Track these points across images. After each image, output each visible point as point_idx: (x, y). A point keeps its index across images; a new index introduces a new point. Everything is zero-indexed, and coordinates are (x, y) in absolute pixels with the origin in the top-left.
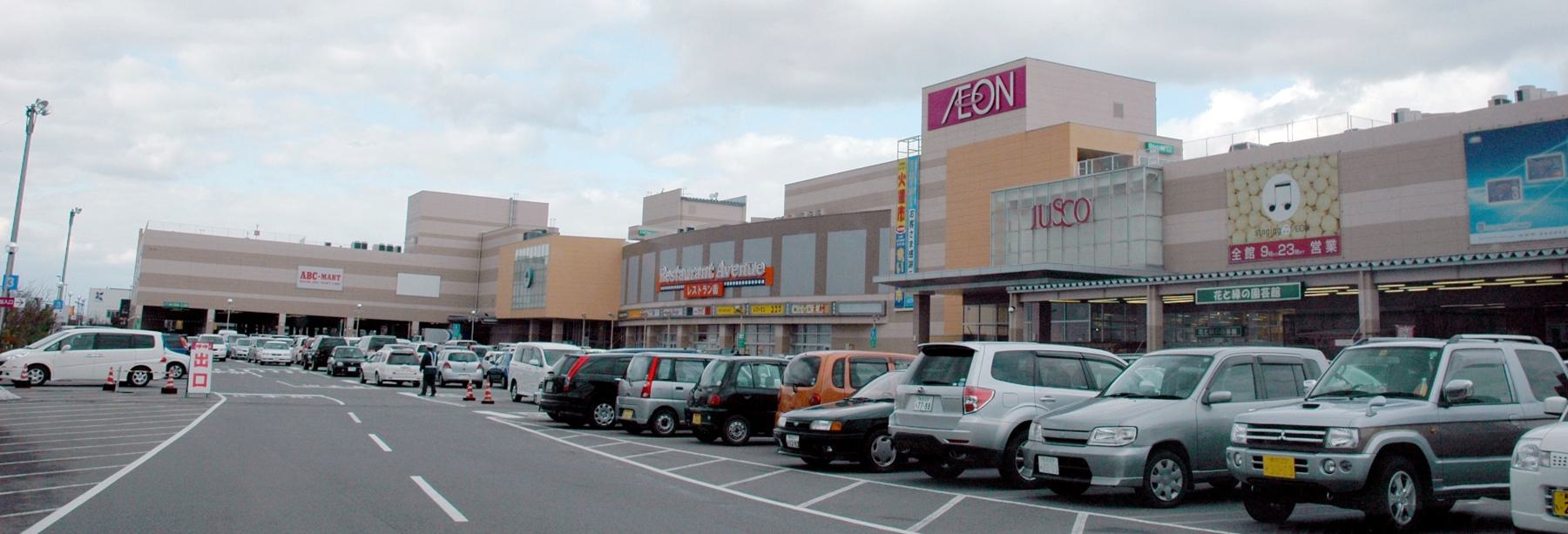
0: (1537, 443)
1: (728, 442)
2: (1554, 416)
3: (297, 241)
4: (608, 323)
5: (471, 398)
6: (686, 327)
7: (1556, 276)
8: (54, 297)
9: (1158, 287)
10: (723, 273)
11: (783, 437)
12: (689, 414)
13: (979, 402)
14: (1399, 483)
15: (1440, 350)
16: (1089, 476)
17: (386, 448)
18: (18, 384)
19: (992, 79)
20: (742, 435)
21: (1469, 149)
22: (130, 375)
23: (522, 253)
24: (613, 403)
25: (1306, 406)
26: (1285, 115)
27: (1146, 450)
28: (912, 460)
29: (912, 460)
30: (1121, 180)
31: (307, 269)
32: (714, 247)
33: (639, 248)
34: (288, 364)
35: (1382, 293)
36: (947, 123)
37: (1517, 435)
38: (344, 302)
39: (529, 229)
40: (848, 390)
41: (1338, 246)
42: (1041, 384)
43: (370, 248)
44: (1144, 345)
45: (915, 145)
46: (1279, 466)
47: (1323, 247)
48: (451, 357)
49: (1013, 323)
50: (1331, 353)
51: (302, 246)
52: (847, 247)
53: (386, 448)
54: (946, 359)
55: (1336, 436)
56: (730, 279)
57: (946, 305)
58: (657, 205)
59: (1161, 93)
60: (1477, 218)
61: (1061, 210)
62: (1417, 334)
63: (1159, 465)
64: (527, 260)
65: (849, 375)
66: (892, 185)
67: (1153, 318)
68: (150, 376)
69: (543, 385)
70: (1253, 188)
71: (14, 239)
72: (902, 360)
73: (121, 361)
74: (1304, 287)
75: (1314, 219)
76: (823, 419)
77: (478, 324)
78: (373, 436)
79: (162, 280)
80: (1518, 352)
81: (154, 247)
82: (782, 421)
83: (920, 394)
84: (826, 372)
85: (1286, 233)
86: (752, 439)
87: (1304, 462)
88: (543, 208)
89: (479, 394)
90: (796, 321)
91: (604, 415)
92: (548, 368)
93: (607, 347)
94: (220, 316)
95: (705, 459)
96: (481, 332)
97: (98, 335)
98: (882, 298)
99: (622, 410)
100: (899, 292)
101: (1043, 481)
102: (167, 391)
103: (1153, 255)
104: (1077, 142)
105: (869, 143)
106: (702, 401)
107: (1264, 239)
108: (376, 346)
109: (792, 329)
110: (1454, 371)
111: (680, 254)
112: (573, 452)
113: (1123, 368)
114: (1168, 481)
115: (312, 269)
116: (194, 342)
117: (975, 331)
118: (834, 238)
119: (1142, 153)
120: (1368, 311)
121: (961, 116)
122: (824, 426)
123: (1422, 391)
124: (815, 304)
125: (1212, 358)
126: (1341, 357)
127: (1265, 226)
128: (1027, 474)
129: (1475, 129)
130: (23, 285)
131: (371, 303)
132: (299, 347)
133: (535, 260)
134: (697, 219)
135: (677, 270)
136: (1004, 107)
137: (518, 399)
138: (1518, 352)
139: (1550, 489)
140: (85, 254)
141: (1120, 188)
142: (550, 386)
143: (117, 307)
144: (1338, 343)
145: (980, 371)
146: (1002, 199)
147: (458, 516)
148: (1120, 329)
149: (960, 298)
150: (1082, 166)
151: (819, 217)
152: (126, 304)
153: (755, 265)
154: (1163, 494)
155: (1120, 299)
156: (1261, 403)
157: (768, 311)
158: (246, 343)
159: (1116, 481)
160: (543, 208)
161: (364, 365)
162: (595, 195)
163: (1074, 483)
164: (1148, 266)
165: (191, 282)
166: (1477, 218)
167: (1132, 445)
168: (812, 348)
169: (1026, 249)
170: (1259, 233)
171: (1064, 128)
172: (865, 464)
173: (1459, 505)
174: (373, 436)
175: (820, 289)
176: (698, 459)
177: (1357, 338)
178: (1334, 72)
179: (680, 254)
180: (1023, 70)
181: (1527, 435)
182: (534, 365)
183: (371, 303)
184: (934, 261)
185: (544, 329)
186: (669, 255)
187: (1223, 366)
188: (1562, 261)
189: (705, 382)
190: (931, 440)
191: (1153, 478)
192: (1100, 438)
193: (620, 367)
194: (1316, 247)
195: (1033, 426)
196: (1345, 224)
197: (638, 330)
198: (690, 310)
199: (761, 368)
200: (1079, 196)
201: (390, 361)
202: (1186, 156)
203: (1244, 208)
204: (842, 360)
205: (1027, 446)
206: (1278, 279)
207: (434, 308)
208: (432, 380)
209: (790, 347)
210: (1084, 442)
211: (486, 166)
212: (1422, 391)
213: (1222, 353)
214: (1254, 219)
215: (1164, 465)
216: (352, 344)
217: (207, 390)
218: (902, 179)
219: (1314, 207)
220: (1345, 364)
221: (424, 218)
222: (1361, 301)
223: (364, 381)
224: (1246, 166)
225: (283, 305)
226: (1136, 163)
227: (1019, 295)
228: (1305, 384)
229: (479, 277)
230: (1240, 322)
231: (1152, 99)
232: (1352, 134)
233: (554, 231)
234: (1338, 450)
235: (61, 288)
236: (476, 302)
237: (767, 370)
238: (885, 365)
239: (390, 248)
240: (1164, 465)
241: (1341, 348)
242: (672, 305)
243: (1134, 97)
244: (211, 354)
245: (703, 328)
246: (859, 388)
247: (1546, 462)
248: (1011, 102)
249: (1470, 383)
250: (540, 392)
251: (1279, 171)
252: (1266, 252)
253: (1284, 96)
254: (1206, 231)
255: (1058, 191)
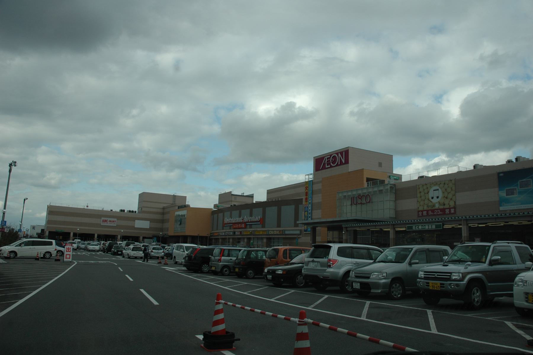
0: (523, 278)
1: (247, 278)
2: (528, 269)
3: (101, 209)
4: (206, 237)
5: (160, 263)
6: (233, 238)
7: (529, 221)
8: (18, 228)
9: (394, 225)
10: (246, 220)
11: (266, 276)
12: (234, 268)
13: (333, 264)
14: (476, 291)
15: (490, 246)
16: (371, 289)
17: (131, 280)
18: (6, 258)
19: (337, 154)
20: (252, 275)
21: (499, 177)
22: (44, 255)
23: (177, 213)
24: (208, 264)
25: (444, 265)
26: (437, 166)
27: (390, 280)
28: (310, 284)
29: (310, 284)
30: (381, 188)
31: (104, 219)
32: (243, 211)
33: (217, 212)
34: (98, 251)
35: (470, 227)
36: (322, 169)
37: (516, 275)
38: (117, 230)
39: (180, 205)
40: (288, 260)
41: (455, 211)
42: (354, 258)
43: (126, 211)
44: (389, 244)
45: (311, 176)
46: (434, 285)
47: (450, 211)
48: (154, 249)
49: (344, 237)
50: (452, 247)
51: (103, 211)
52: (288, 211)
53: (131, 280)
54: (322, 249)
55: (454, 276)
56: (248, 222)
57: (321, 231)
58: (224, 197)
59: (395, 159)
60: (502, 201)
61: (361, 199)
62: (482, 241)
63: (394, 285)
64: (179, 215)
65: (289, 255)
66: (303, 190)
67: (392, 236)
68: (51, 255)
69: (184, 258)
70: (426, 191)
71: (5, 208)
72: (307, 250)
73: (41, 250)
74: (443, 225)
75: (447, 202)
76: (280, 269)
77: (163, 237)
78: (127, 276)
79: (55, 222)
80: (516, 247)
81: (52, 211)
82: (266, 270)
83: (313, 261)
84: (281, 254)
85: (437, 206)
86: (256, 276)
87: (443, 284)
88: (185, 198)
89: (163, 261)
90: (271, 236)
91: (205, 268)
92: (186, 252)
93: (206, 245)
94: (75, 235)
95: (240, 283)
96: (164, 240)
97: (33, 241)
98: (300, 228)
99: (211, 267)
100: (306, 227)
101: (355, 291)
102: (58, 260)
103: (392, 214)
104: (366, 175)
105: (295, 176)
106: (239, 264)
107: (430, 208)
108: (128, 245)
109: (269, 239)
110: (494, 253)
111: (231, 214)
112: (195, 281)
113: (382, 252)
114: (397, 291)
115: (106, 219)
116: (66, 243)
117: (331, 240)
118: (283, 208)
119: (388, 179)
120: (465, 233)
121: (327, 167)
122: (280, 272)
123: (484, 260)
124: (277, 231)
125: (412, 249)
126: (456, 249)
127: (430, 204)
128: (349, 289)
129: (501, 171)
130: (8, 224)
131: (126, 230)
132: (102, 245)
133: (182, 215)
134: (236, 202)
135: (230, 219)
136: (341, 164)
137: (176, 263)
138: (516, 247)
139: (527, 294)
140: (29, 211)
141: (381, 191)
142: (187, 258)
143: (40, 232)
144: (455, 244)
145: (333, 254)
146: (340, 195)
147: (156, 303)
148: (381, 239)
149: (327, 229)
150: (368, 183)
151: (279, 199)
152: (43, 230)
153: (257, 217)
154: (395, 295)
155: (381, 229)
156: (429, 264)
157: (261, 233)
158: (84, 244)
159: (380, 291)
160: (185, 198)
161: (124, 251)
162: (202, 193)
163: (366, 291)
164: (390, 217)
165: (64, 223)
166: (502, 201)
167: (385, 279)
168: (276, 246)
169: (349, 212)
170: (428, 206)
171: (362, 171)
172: (294, 286)
173: (496, 299)
174: (127, 276)
175: (279, 225)
176: (237, 283)
177: (462, 243)
178: (453, 152)
179: (231, 214)
180: (348, 150)
181: (519, 275)
182: (181, 251)
183: (126, 230)
184: (318, 216)
185: (185, 239)
186: (227, 214)
187: (416, 251)
188: (531, 216)
189: (240, 257)
190: (316, 277)
191: (392, 290)
192: (374, 276)
193: (211, 251)
194: (447, 211)
195: (351, 272)
196: (457, 203)
197: (217, 239)
198: (234, 233)
199: (259, 252)
200: (367, 194)
201: (133, 250)
202: (403, 180)
203: (423, 198)
204: (286, 250)
205: (349, 279)
206: (434, 222)
207: (147, 232)
208: (147, 256)
209: (268, 245)
210: (368, 278)
211: (164, 183)
212: (484, 260)
213: (416, 247)
214: (426, 202)
215: (396, 285)
216: (120, 244)
217: (70, 260)
218: (306, 188)
219: (447, 198)
220: (457, 251)
221: (144, 201)
222: (463, 229)
223: (124, 257)
224: (424, 183)
225: (96, 231)
226: (386, 182)
227: (346, 228)
228: (444, 258)
229: (163, 221)
230: (421, 237)
231: (392, 161)
232: (460, 173)
233: (188, 206)
234: (455, 280)
235: (21, 225)
236: (162, 230)
237: (261, 253)
238: (300, 252)
239: (133, 212)
240: (396, 285)
241: (456, 246)
242: (228, 231)
243: (385, 160)
244: (72, 248)
245: (239, 239)
246: (292, 259)
247: (525, 284)
248: (344, 162)
249: (499, 257)
250: (183, 261)
251: (435, 185)
252: (430, 213)
253: (436, 160)
254: (409, 205)
255: (360, 192)
